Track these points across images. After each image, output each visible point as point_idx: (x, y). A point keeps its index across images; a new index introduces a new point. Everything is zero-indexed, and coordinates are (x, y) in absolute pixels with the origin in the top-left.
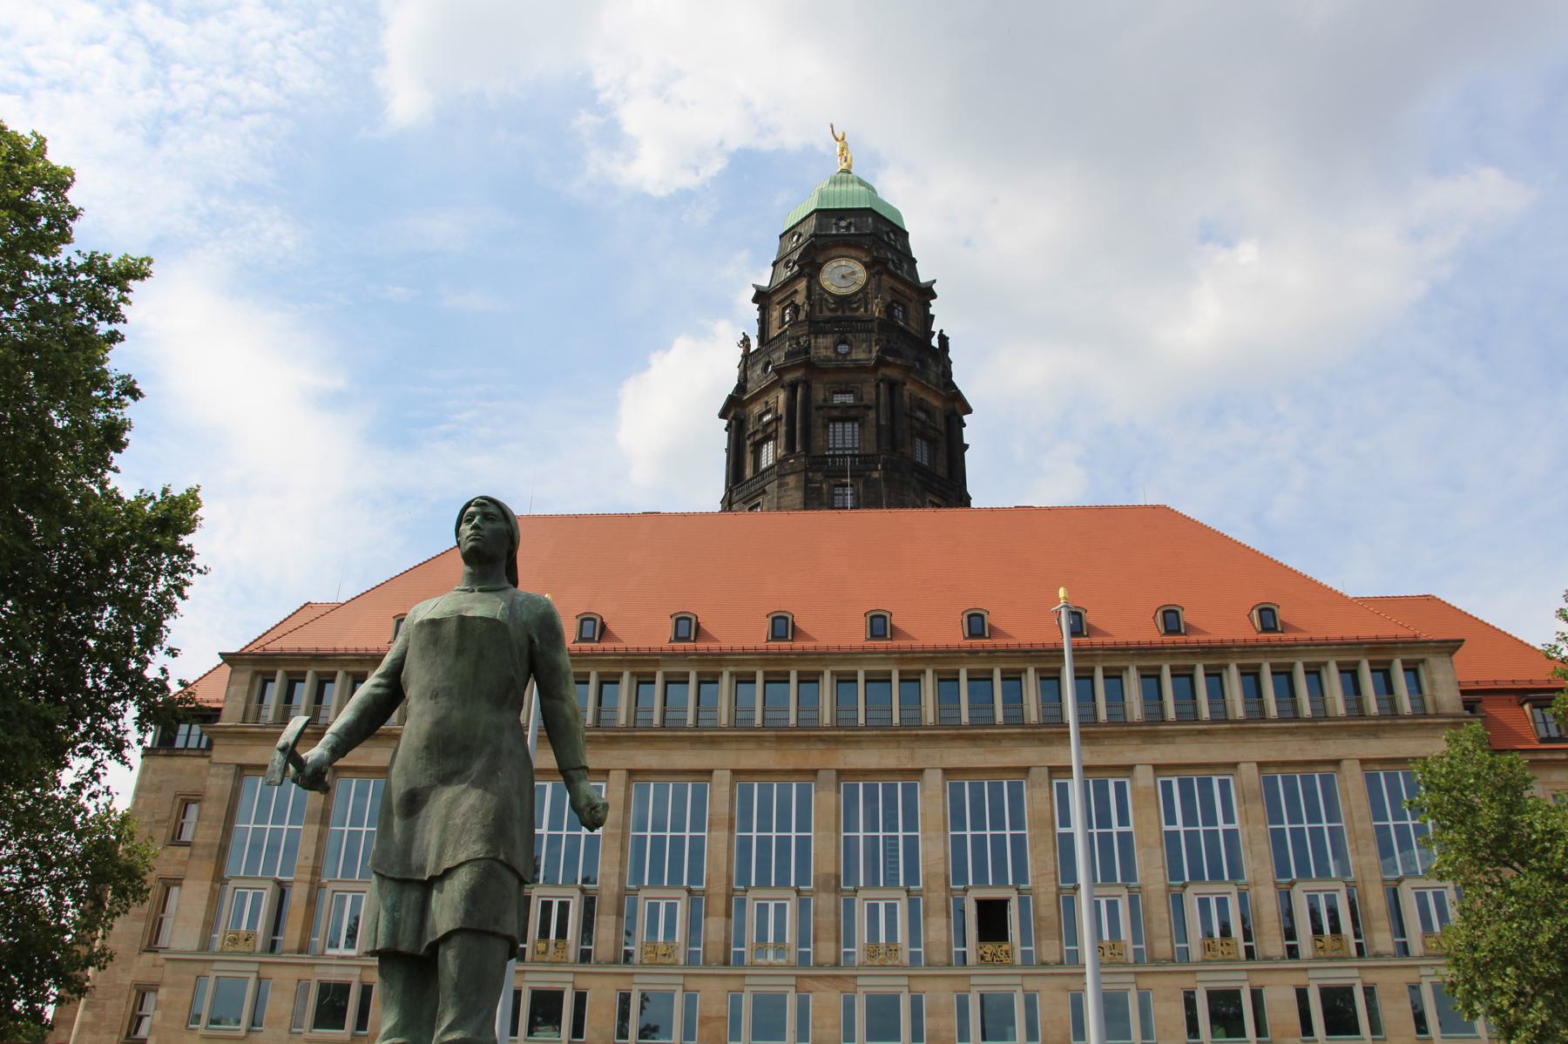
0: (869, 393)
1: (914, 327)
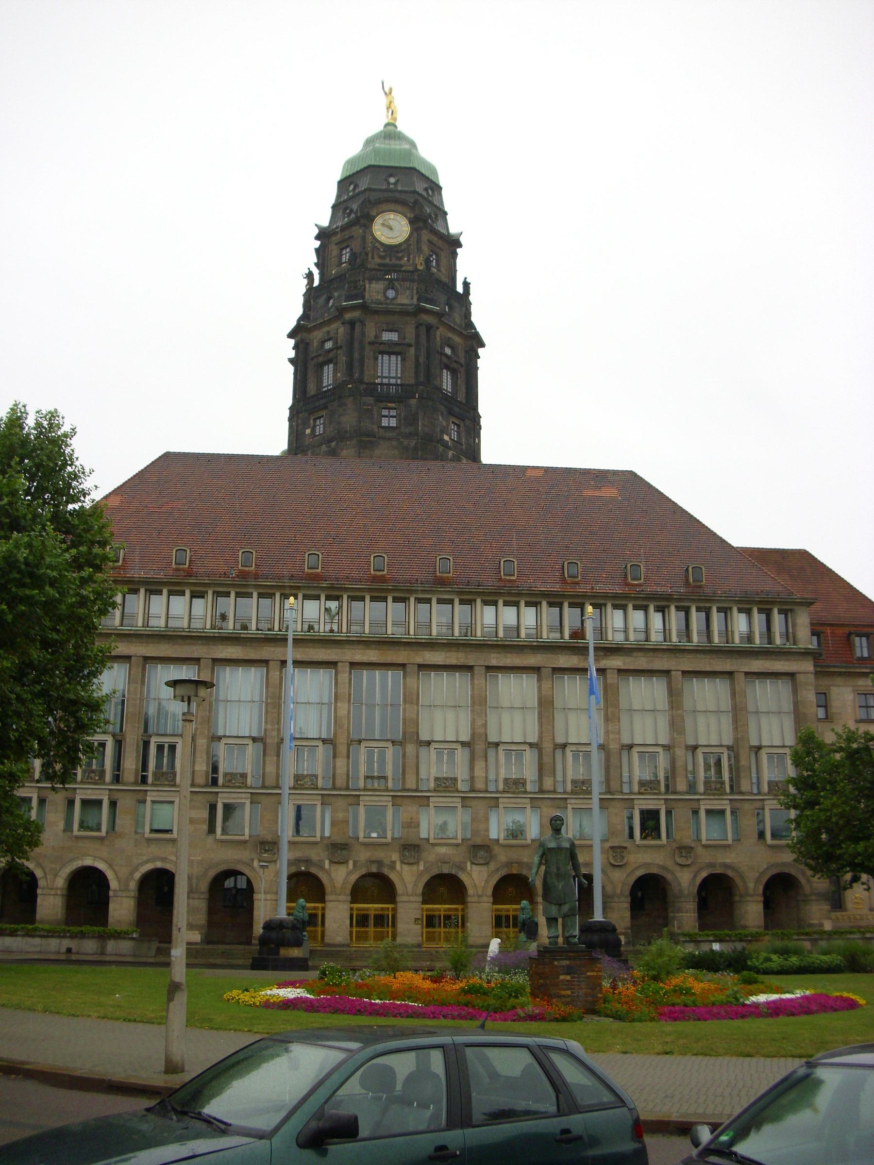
0: (410, 333)
1: (444, 279)
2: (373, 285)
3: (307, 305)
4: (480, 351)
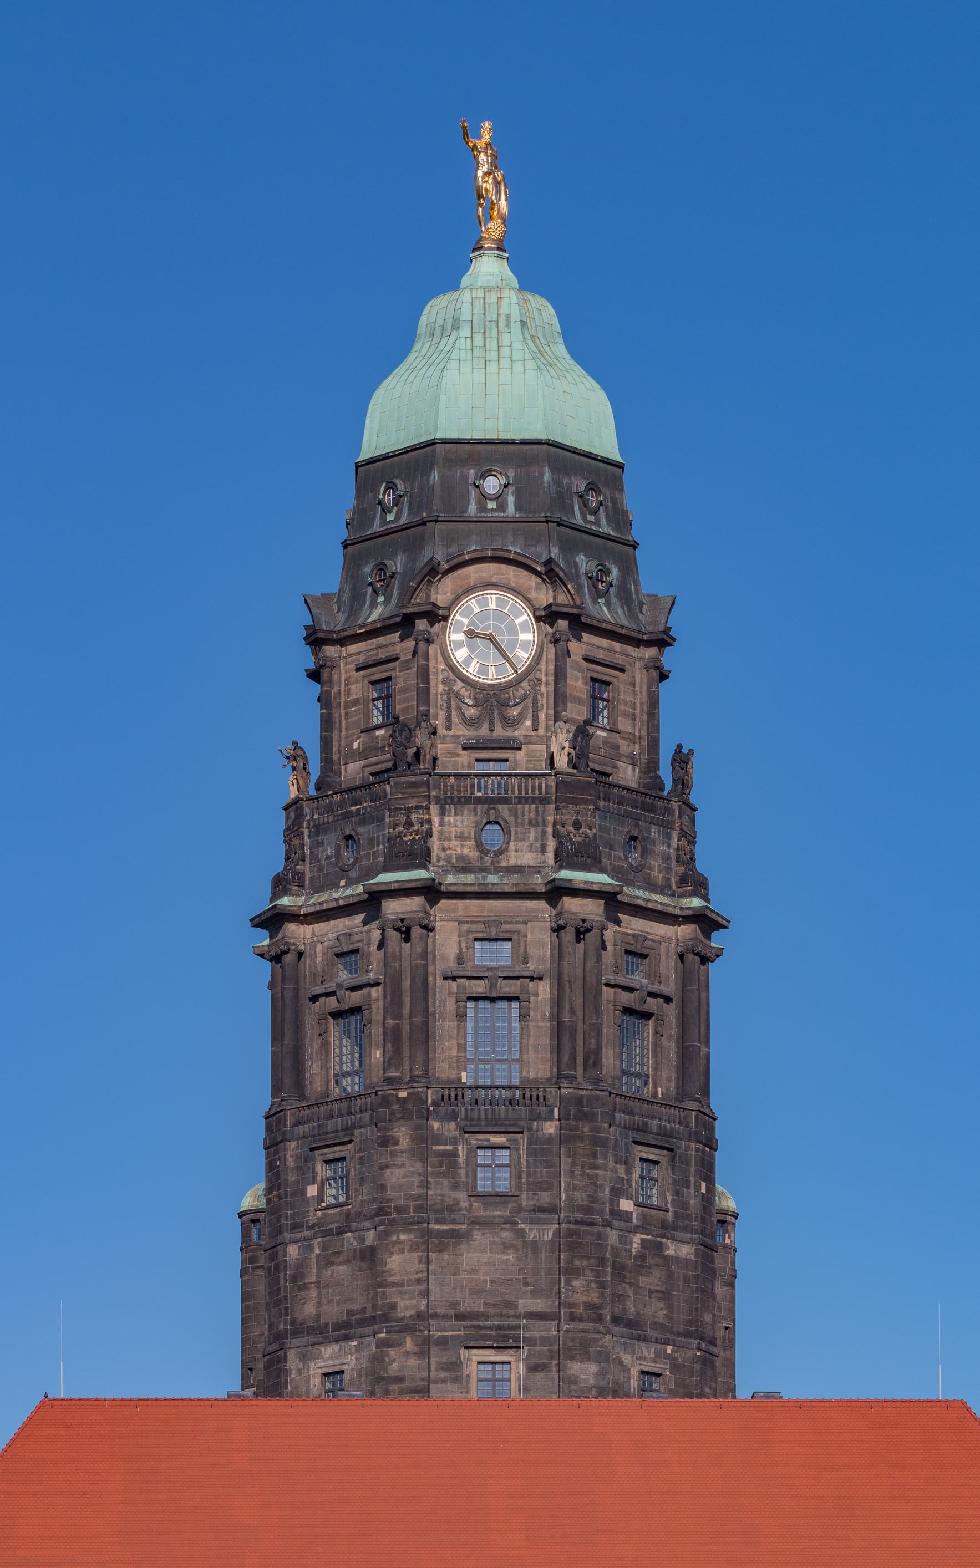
2: (449, 819)
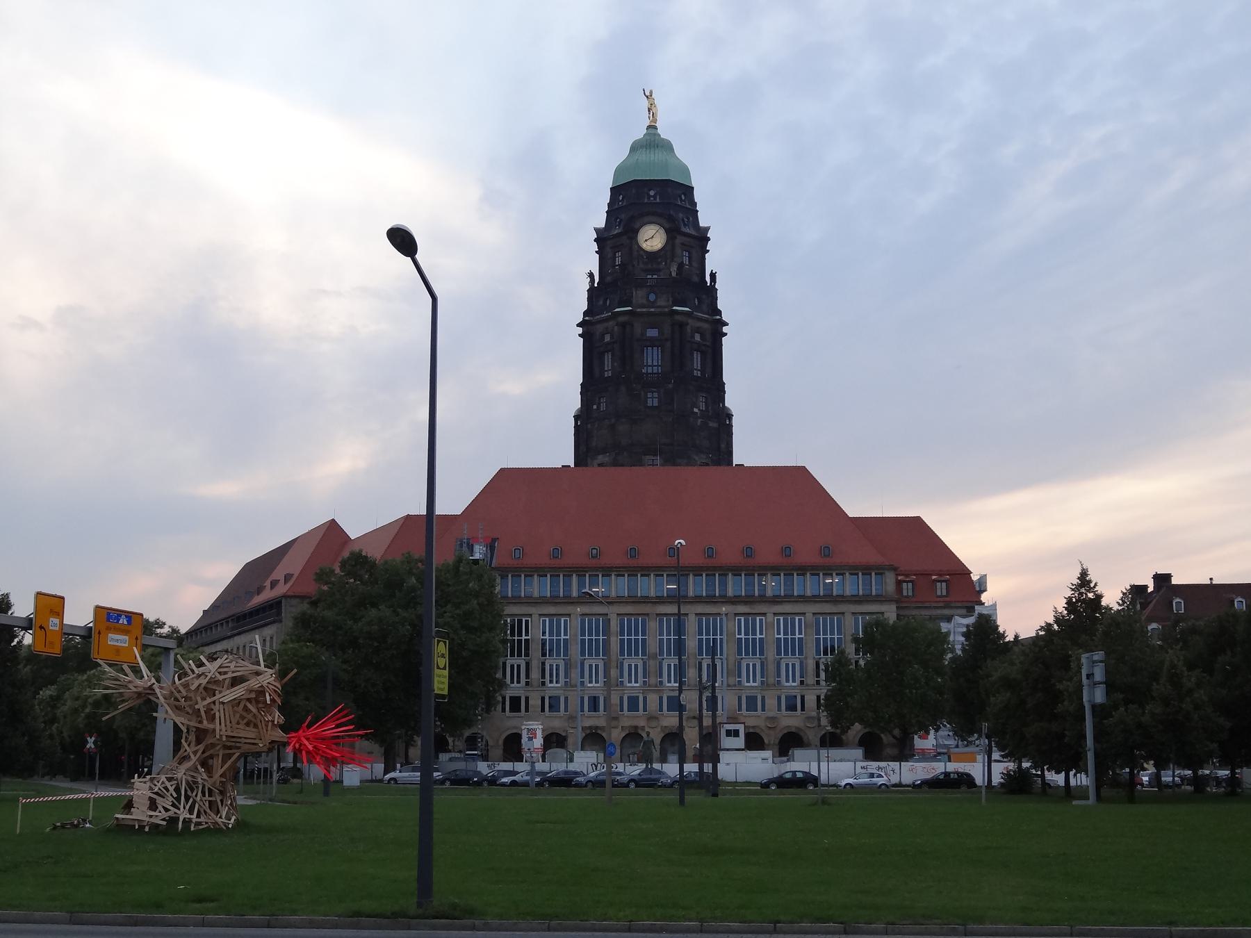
1: (696, 279)
3: (590, 299)
4: (725, 329)
